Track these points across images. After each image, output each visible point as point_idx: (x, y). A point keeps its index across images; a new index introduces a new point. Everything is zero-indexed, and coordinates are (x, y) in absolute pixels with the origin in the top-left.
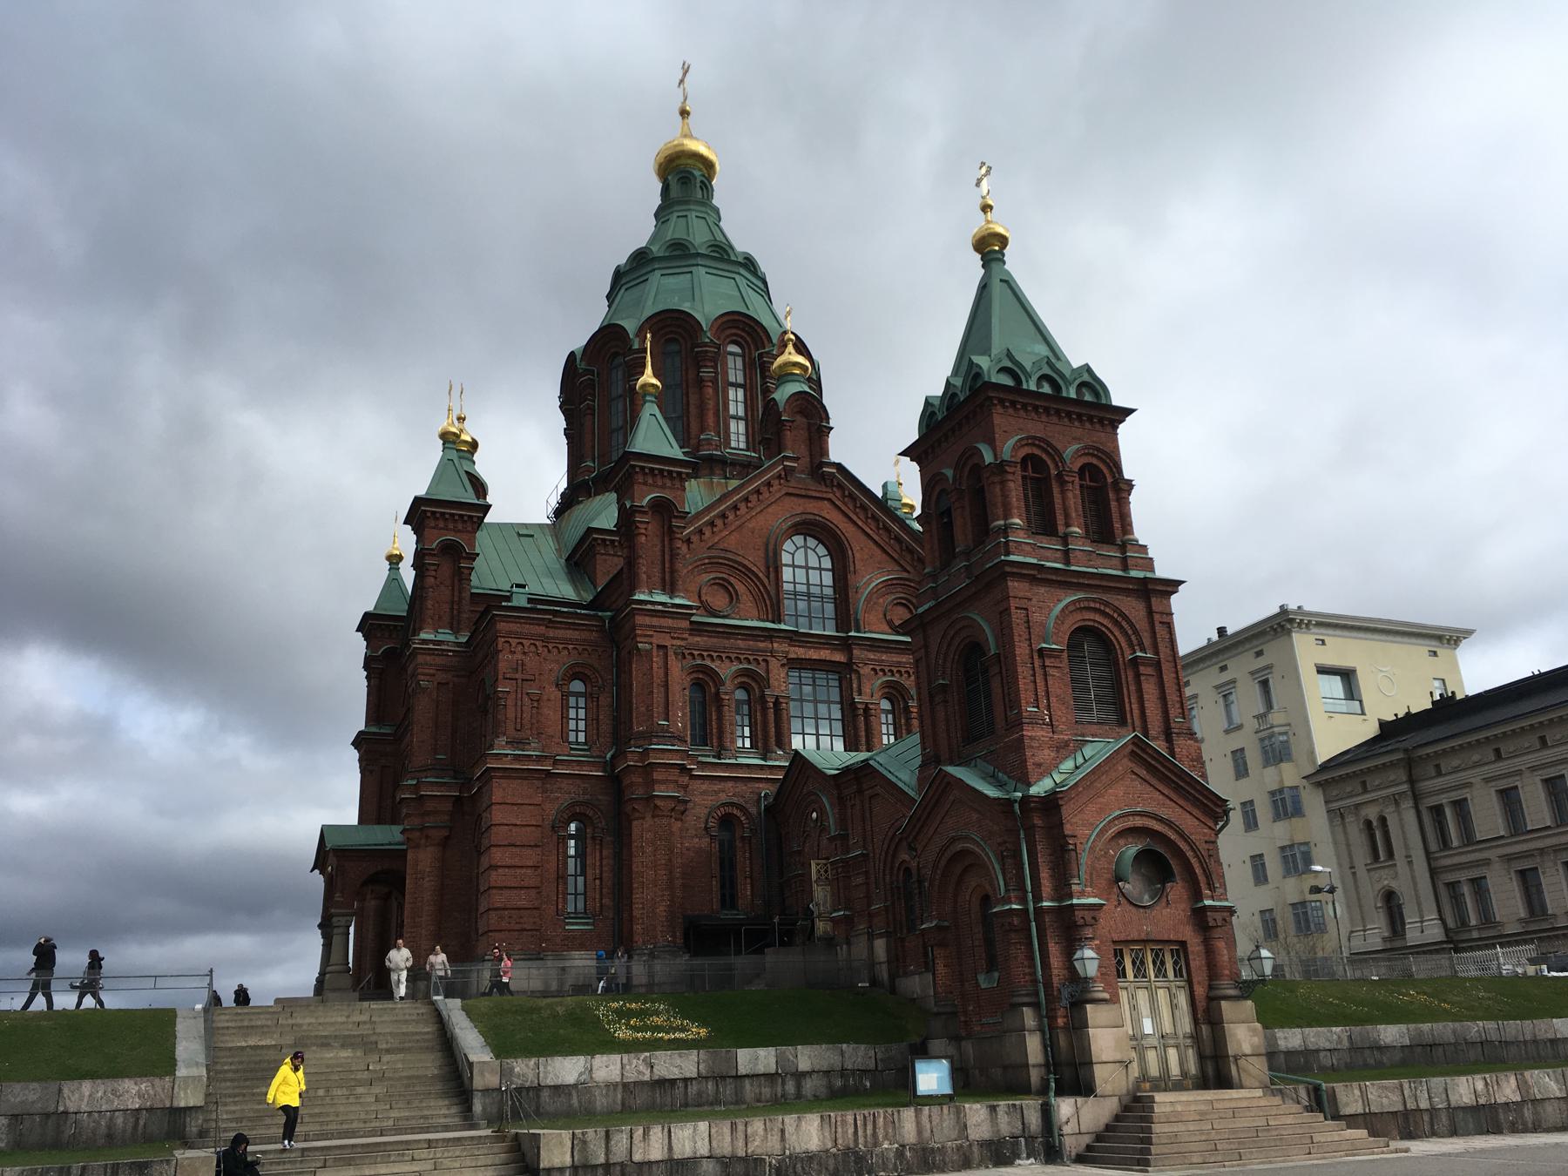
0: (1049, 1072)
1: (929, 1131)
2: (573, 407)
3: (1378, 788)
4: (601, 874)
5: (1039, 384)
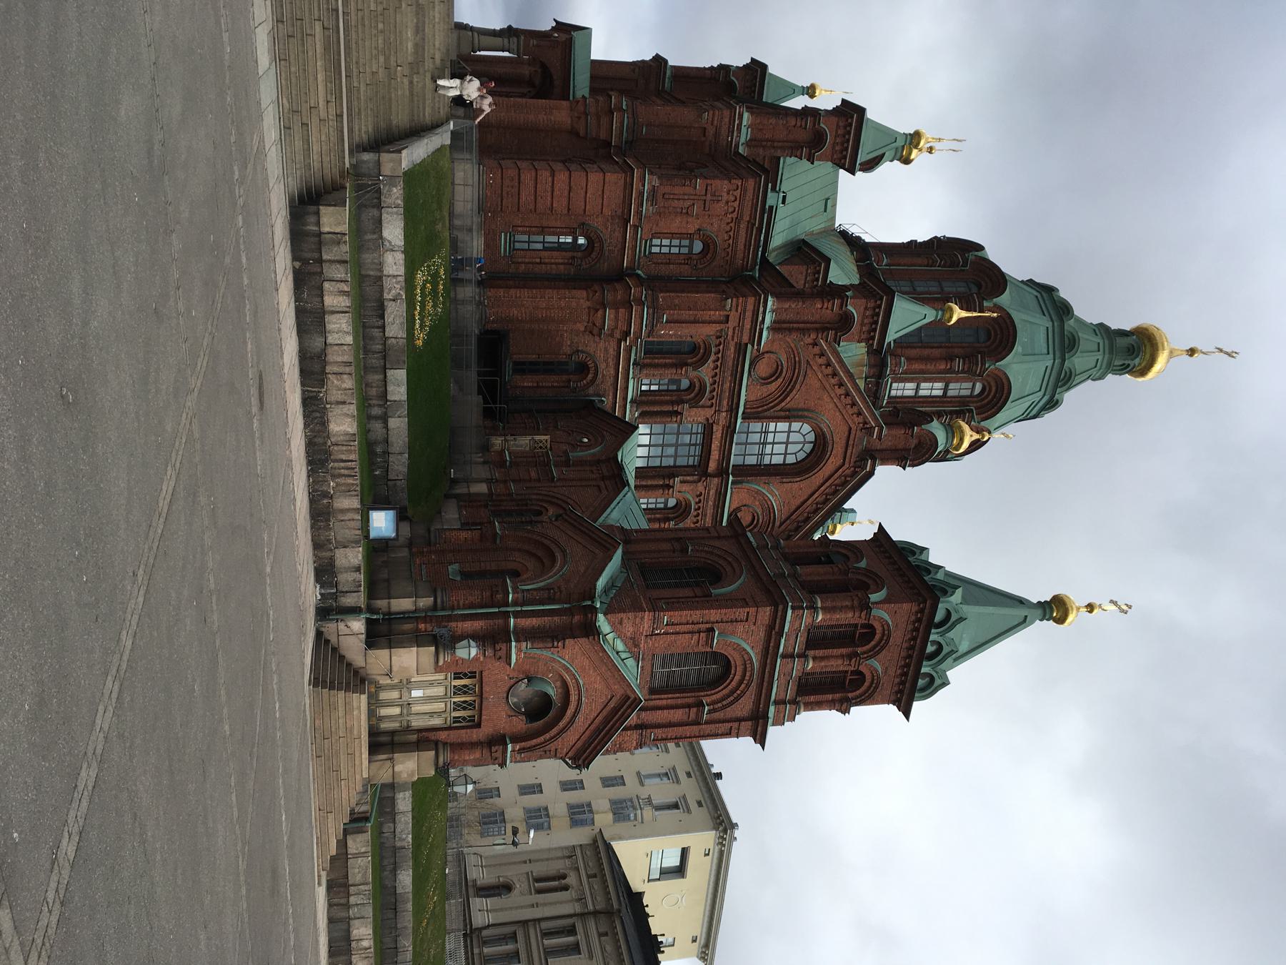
0: (384, 615)
1: (342, 518)
2: (935, 248)
3: (591, 887)
4: (545, 263)
5: (934, 642)
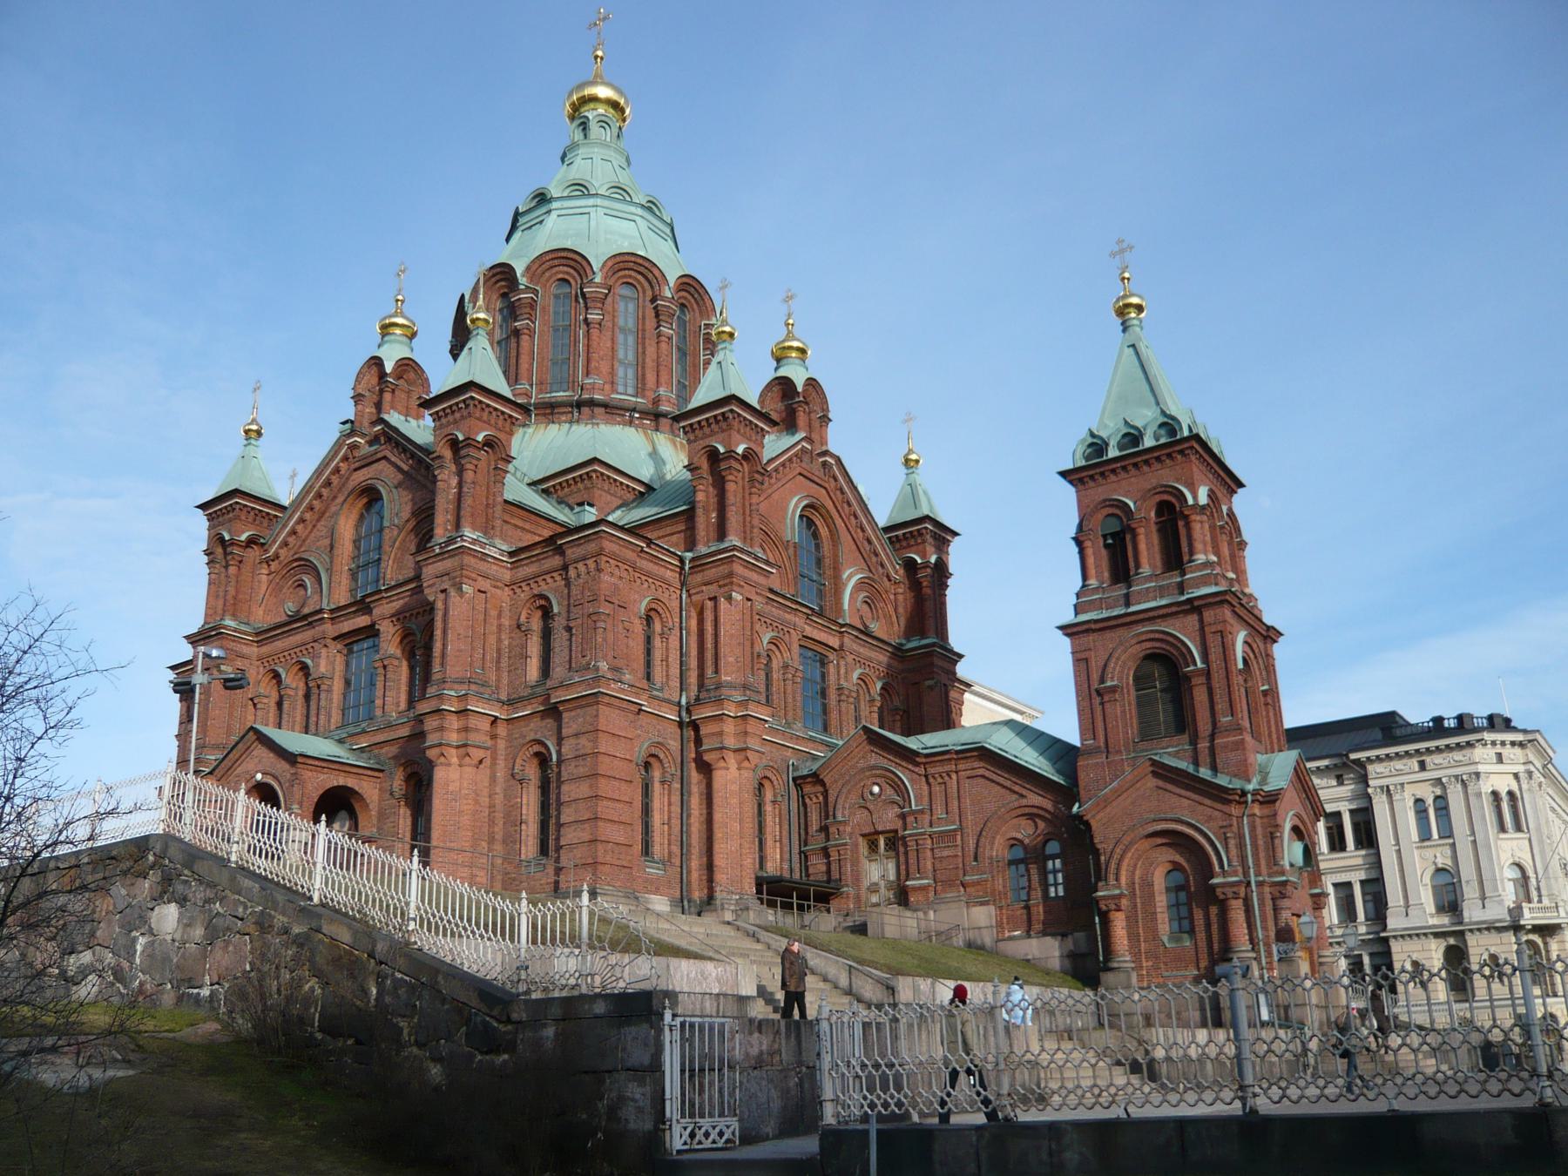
4: (669, 819)
